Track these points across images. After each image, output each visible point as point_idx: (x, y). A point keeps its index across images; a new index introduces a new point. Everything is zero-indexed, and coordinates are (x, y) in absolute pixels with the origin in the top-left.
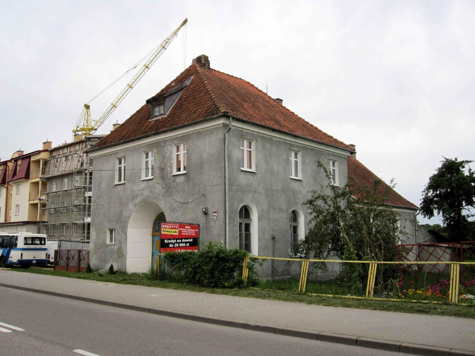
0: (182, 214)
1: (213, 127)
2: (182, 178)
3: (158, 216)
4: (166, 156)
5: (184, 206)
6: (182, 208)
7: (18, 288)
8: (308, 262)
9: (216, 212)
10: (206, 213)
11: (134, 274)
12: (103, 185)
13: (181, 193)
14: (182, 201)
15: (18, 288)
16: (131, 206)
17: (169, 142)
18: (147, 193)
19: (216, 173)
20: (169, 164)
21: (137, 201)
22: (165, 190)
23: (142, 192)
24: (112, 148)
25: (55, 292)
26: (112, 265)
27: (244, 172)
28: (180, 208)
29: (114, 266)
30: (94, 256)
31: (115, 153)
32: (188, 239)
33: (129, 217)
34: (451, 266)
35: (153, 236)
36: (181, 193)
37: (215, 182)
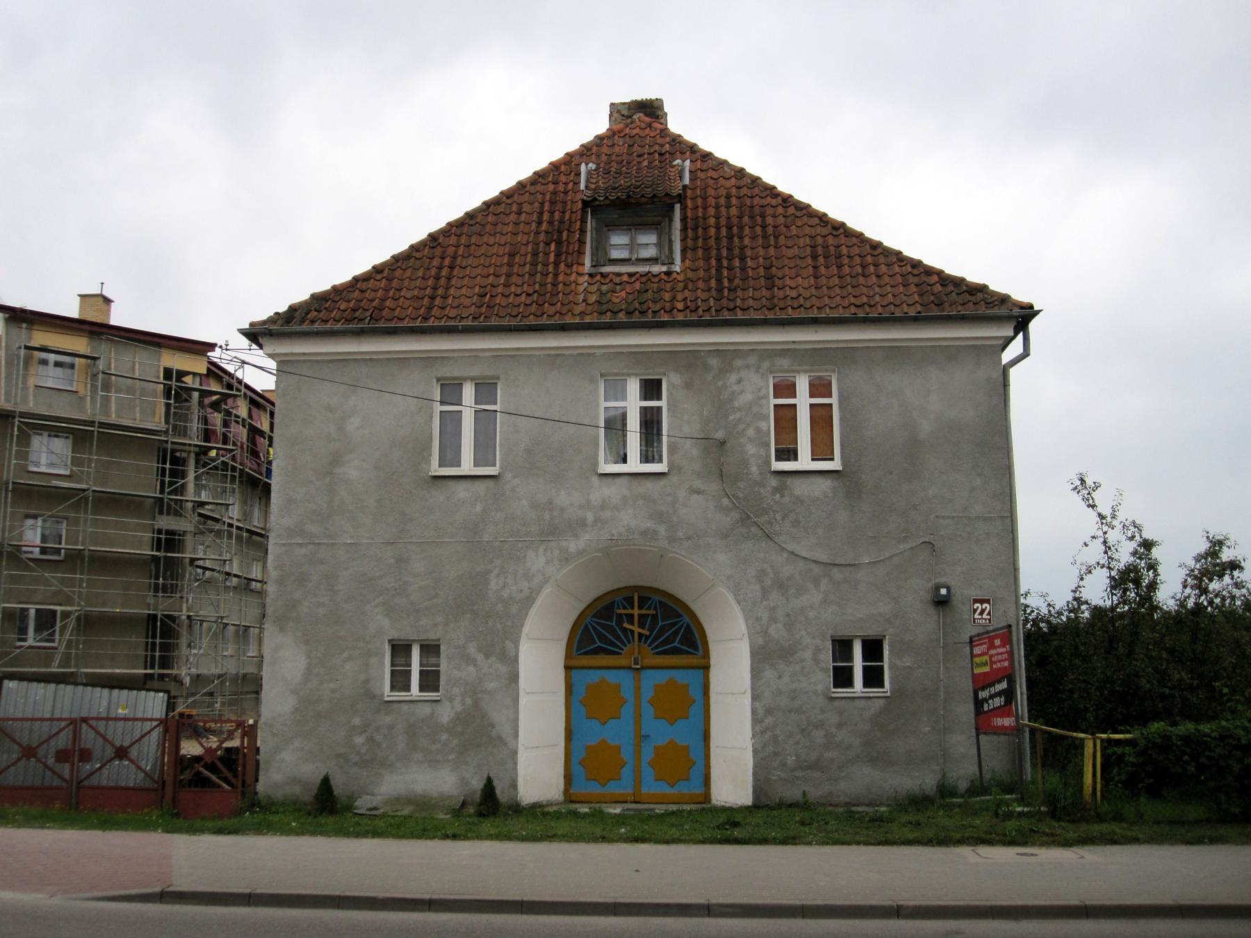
0: (825, 601)
1: (958, 343)
2: (824, 485)
3: (596, 600)
4: (736, 404)
5: (837, 574)
6: (824, 581)
7: (250, 899)
8: (1098, 742)
9: (988, 601)
10: (941, 603)
11: (535, 806)
12: (354, 470)
13: (820, 531)
14: (823, 556)
15: (250, 899)
16: (537, 561)
17: (752, 360)
18: (629, 520)
19: (978, 481)
20: (751, 432)
21: (572, 546)
22: (735, 515)
23: (607, 514)
24: (427, 338)
25: (583, 899)
26: (489, 781)
27: (610, 480)
28: (816, 582)
29: (496, 783)
30: (297, 743)
31: (429, 360)
32: (992, 684)
33: (529, 601)
34: (1082, 747)
35: (568, 668)
36: (820, 531)
37: (977, 509)
